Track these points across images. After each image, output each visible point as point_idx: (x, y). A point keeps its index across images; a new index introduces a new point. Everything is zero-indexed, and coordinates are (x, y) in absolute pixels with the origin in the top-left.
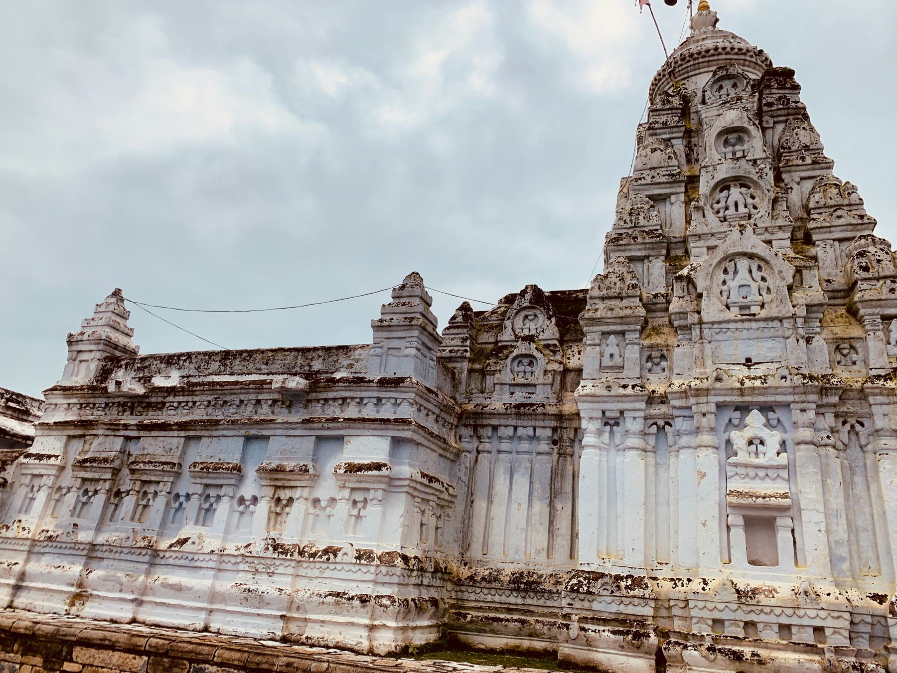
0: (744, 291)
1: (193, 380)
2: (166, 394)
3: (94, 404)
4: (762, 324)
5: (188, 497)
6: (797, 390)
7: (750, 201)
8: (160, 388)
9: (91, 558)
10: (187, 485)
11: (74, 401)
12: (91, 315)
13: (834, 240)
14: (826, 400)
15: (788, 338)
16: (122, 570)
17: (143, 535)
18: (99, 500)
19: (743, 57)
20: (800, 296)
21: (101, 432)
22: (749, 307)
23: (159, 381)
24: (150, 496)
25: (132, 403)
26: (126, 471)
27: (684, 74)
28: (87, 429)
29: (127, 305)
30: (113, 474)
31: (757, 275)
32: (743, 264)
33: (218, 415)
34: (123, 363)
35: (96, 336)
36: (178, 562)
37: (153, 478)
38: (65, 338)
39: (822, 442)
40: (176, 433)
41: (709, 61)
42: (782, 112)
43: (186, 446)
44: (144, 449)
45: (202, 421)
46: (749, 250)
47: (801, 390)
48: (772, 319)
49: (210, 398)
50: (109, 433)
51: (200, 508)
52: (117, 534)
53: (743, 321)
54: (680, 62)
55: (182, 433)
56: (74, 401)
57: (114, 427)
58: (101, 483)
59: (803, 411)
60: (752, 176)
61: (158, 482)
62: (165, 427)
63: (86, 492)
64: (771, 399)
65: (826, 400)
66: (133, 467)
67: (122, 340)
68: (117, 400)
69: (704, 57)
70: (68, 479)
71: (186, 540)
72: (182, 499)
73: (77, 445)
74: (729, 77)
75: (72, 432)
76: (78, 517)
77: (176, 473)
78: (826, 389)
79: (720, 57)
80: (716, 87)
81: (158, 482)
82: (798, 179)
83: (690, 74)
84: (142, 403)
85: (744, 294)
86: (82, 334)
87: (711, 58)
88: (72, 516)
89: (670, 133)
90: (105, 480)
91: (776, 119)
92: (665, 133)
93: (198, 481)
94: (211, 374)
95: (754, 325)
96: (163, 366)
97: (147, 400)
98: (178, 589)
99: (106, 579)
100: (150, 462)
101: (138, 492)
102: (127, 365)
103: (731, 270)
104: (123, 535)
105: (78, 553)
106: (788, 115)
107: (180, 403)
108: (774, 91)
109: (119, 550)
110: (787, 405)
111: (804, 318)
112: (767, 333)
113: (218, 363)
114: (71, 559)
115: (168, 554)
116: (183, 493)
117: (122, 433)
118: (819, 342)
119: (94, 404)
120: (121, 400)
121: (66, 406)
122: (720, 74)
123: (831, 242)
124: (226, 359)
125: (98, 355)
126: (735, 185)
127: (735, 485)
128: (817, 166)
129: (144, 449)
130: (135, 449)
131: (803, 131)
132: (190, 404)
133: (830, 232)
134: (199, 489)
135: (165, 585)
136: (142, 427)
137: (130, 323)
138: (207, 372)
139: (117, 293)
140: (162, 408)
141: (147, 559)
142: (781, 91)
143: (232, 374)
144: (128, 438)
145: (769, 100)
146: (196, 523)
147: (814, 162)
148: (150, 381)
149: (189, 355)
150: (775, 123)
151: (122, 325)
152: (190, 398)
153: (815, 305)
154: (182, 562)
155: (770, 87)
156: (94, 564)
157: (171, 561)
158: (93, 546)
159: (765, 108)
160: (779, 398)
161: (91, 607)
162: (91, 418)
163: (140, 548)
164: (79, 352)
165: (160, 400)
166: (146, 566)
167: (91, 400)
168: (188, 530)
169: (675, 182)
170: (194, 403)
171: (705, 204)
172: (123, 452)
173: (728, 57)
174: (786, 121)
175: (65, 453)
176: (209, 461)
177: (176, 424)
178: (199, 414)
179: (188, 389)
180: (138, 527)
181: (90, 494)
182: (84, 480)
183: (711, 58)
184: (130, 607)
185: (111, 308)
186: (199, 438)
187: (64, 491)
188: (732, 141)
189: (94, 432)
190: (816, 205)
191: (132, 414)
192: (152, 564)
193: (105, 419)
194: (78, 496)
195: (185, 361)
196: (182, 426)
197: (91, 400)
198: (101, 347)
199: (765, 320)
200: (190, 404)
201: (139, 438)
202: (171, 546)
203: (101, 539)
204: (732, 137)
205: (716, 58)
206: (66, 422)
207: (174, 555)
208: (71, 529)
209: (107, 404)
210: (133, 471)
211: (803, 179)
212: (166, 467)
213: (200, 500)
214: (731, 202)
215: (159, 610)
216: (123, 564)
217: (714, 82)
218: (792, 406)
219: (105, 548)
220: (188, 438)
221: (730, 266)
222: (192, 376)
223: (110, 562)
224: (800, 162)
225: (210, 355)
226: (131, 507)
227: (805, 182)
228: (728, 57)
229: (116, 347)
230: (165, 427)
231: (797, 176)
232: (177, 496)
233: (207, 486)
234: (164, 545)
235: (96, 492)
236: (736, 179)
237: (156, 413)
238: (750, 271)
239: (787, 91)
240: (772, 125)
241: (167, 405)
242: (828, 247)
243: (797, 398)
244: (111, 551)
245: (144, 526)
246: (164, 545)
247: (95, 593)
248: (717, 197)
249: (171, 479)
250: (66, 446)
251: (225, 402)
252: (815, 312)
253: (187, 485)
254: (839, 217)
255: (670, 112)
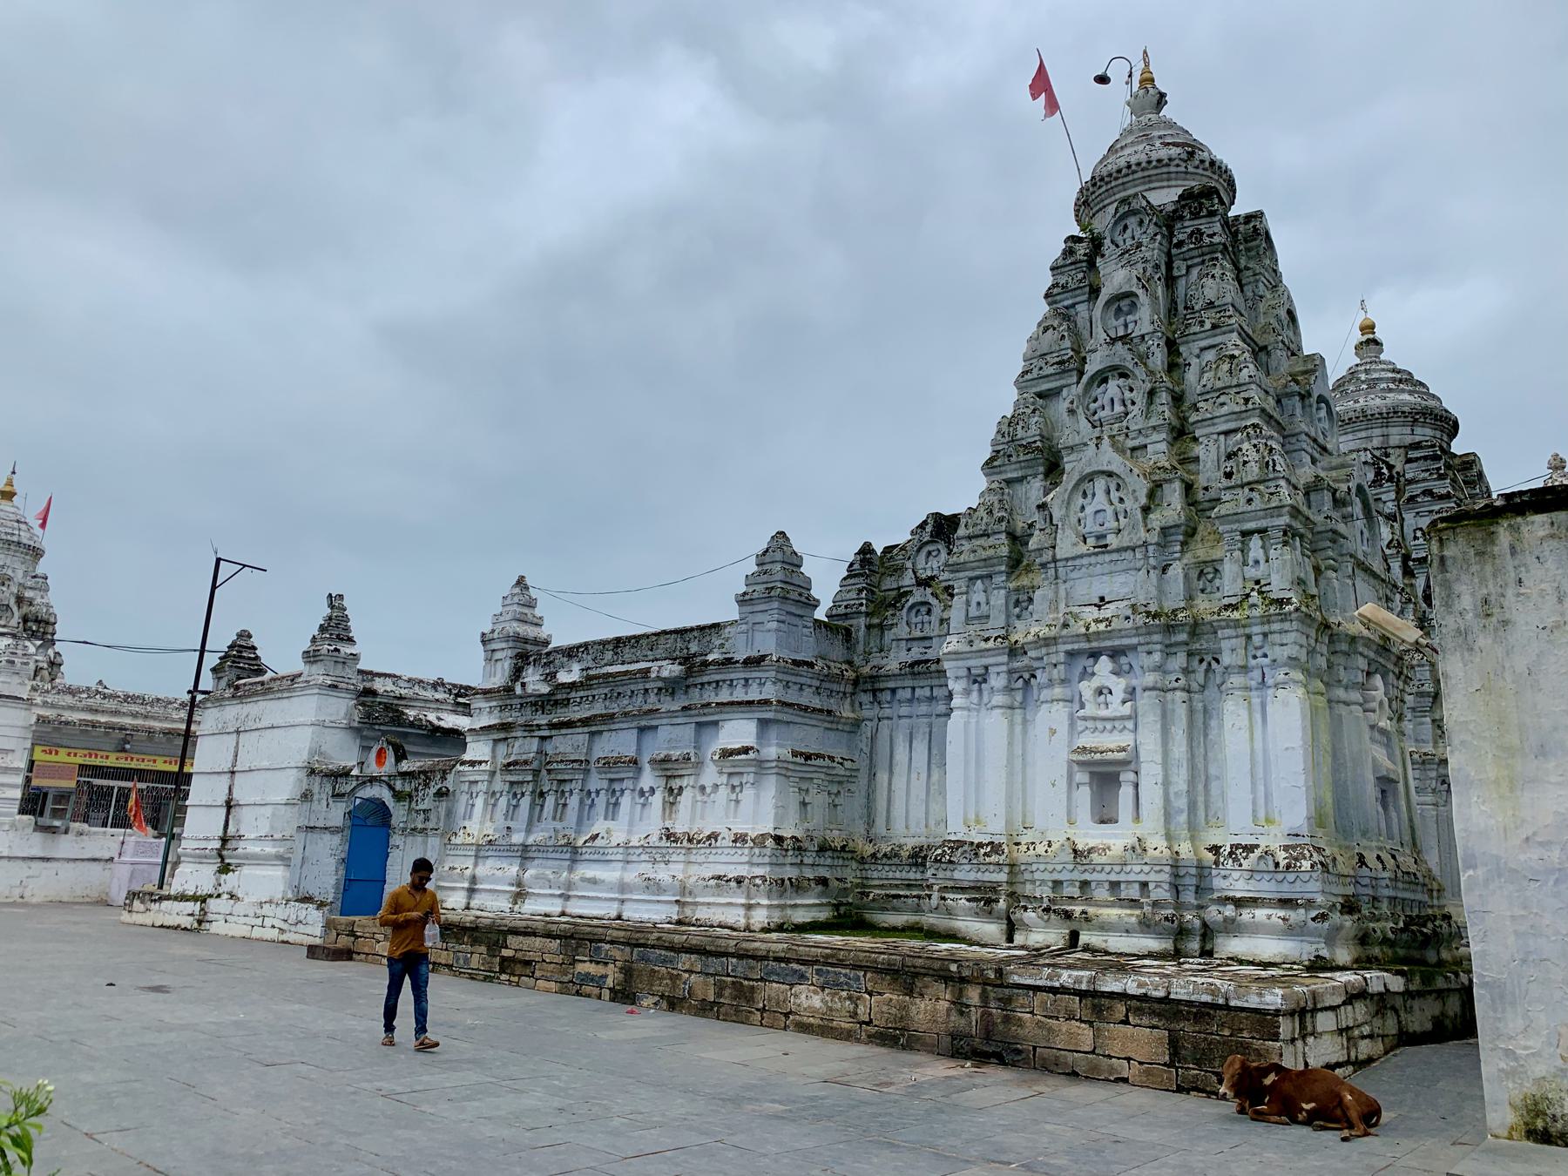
0: (1100, 517)
1: (591, 672)
2: (569, 690)
3: (511, 705)
4: (1115, 556)
5: (598, 792)
6: (1140, 631)
7: (1128, 395)
8: (563, 684)
9: (526, 858)
10: (596, 782)
11: (494, 704)
12: (499, 609)
13: (1219, 434)
14: (1174, 639)
15: (1139, 570)
16: (550, 868)
17: (563, 833)
18: (525, 802)
19: (1165, 170)
20: (1156, 519)
21: (519, 734)
22: (1104, 536)
23: (563, 677)
24: (567, 795)
25: (541, 703)
26: (544, 772)
27: (1098, 203)
28: (507, 732)
29: (533, 593)
30: (534, 776)
31: (1115, 495)
32: (1100, 484)
33: (614, 708)
34: (531, 659)
35: (505, 632)
36: (592, 857)
37: (566, 777)
38: (479, 638)
39: (1170, 686)
40: (580, 730)
41: (1123, 184)
42: (1195, 253)
43: (591, 742)
44: (557, 748)
45: (601, 715)
46: (1105, 468)
47: (1143, 630)
48: (1126, 549)
49: (606, 691)
50: (526, 734)
51: (608, 803)
52: (541, 834)
53: (1096, 554)
54: (1091, 189)
55: (586, 729)
56: (494, 704)
57: (529, 728)
58: (525, 785)
59: (1149, 653)
60: (1127, 364)
61: (571, 780)
62: (569, 724)
63: (515, 795)
64: (1117, 642)
65: (1174, 639)
66: (548, 767)
67: (530, 631)
68: (529, 700)
69: (1116, 179)
70: (499, 784)
71: (597, 835)
72: (593, 795)
73: (502, 749)
74: (1134, 213)
75: (496, 736)
76: (512, 820)
77: (585, 770)
78: (1172, 626)
79: (1136, 176)
80: (1120, 228)
81: (571, 780)
82: (1197, 351)
83: (1106, 202)
84: (550, 701)
85: (1101, 521)
86: (493, 631)
87: (1125, 180)
88: (506, 819)
89: (1072, 297)
90: (528, 782)
91: (1189, 263)
92: (1067, 299)
93: (603, 776)
94: (606, 665)
95: (1107, 558)
96: (565, 659)
97: (553, 698)
98: (594, 882)
99: (537, 877)
100: (562, 761)
101: (556, 791)
102: (535, 660)
103: (1089, 493)
104: (547, 835)
105: (514, 854)
106: (1203, 254)
107: (582, 698)
108: (1187, 223)
109: (545, 849)
110: (1134, 648)
111: (1157, 544)
112: (1120, 566)
113: (611, 653)
114: (509, 860)
115: (584, 850)
116: (593, 790)
117: (536, 733)
118: (1176, 570)
119: (511, 705)
120: (532, 699)
121: (488, 710)
122: (1121, 211)
123: (1215, 436)
124: (617, 647)
125: (509, 653)
126: (1113, 376)
127: (1087, 740)
128: (1218, 331)
129: (557, 748)
130: (549, 748)
131: (1211, 281)
132: (590, 698)
133: (1214, 425)
134: (605, 784)
135: (583, 880)
136: (552, 726)
137: (538, 612)
138: (603, 663)
139: (521, 582)
140: (568, 704)
141: (568, 856)
142: (1196, 222)
143: (623, 664)
144: (543, 738)
145: (1181, 237)
146: (606, 818)
147: (1214, 327)
148: (555, 677)
149: (586, 645)
150: (1189, 268)
151: (530, 616)
152: (589, 693)
153: (1171, 527)
154: (596, 857)
155: (1182, 218)
156: (528, 864)
157: (587, 857)
158: (525, 847)
159: (1174, 251)
160: (1126, 641)
161: (529, 904)
162: (510, 720)
163: (561, 846)
164: (493, 651)
165: (565, 696)
166: (568, 863)
167: (508, 702)
168: (599, 826)
169: (1064, 372)
170: (594, 696)
171: (1078, 407)
172: (539, 752)
173: (1146, 173)
174: (1203, 262)
175: (494, 757)
176: (610, 755)
177: (579, 720)
178: (599, 708)
179: (587, 683)
180: (558, 825)
181: (519, 796)
182: (512, 783)
183: (1125, 180)
184: (559, 901)
185: (516, 599)
186: (600, 732)
187: (498, 795)
188: (1125, 309)
189: (514, 734)
190: (1203, 390)
191: (543, 713)
192: (574, 861)
193: (521, 721)
194: (509, 800)
195: (583, 652)
196: (585, 722)
197: (508, 702)
198: (511, 644)
199: (1118, 550)
200: (590, 698)
201: (551, 737)
202: (585, 842)
203: (530, 841)
204: (1124, 304)
205: (1131, 177)
206: (490, 726)
207: (589, 850)
208: (505, 832)
209: (522, 705)
210: (549, 771)
211: (1202, 350)
212: (576, 765)
213: (607, 795)
214: (1106, 401)
215: (581, 903)
216: (550, 863)
217: (1116, 223)
218: (1139, 648)
219: (534, 849)
220: (592, 734)
221: (1087, 486)
222: (589, 668)
223: (540, 861)
224: (1197, 329)
225: (603, 643)
226: (552, 807)
227: (1206, 352)
228: (1146, 173)
229: (526, 641)
230: (569, 724)
231: (1195, 347)
232: (589, 793)
233: (611, 780)
234: (580, 843)
235: (523, 795)
236: (1113, 368)
237: (563, 710)
238: (1108, 492)
239: (1203, 221)
240: (1184, 272)
241: (572, 701)
242: (1211, 444)
243: (1142, 639)
244: (539, 851)
245: (564, 824)
246: (580, 843)
247: (530, 890)
248: (1094, 395)
249: (582, 776)
250: (493, 751)
251: (619, 694)
252: (1173, 535)
253: (596, 782)
254: (1223, 404)
255: (1073, 267)
